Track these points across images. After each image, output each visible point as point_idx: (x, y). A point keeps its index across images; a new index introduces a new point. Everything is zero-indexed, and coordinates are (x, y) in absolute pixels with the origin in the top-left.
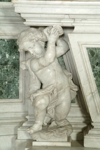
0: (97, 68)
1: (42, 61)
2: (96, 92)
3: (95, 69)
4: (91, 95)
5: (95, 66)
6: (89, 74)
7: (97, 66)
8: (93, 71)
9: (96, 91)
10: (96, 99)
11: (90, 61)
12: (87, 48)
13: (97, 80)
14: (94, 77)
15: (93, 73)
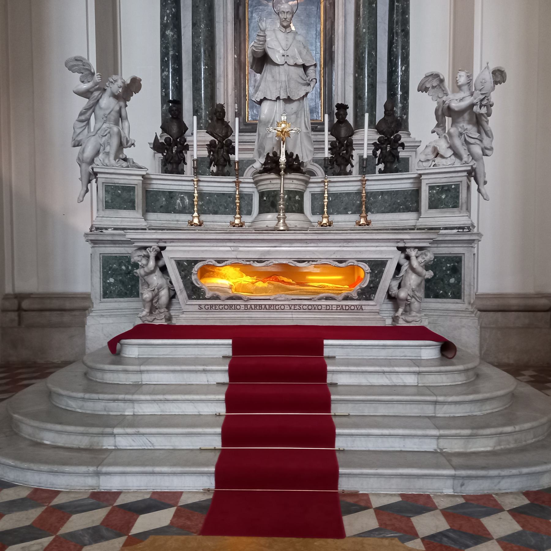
1: (146, 269)
12: (175, 260)
14: (182, 279)
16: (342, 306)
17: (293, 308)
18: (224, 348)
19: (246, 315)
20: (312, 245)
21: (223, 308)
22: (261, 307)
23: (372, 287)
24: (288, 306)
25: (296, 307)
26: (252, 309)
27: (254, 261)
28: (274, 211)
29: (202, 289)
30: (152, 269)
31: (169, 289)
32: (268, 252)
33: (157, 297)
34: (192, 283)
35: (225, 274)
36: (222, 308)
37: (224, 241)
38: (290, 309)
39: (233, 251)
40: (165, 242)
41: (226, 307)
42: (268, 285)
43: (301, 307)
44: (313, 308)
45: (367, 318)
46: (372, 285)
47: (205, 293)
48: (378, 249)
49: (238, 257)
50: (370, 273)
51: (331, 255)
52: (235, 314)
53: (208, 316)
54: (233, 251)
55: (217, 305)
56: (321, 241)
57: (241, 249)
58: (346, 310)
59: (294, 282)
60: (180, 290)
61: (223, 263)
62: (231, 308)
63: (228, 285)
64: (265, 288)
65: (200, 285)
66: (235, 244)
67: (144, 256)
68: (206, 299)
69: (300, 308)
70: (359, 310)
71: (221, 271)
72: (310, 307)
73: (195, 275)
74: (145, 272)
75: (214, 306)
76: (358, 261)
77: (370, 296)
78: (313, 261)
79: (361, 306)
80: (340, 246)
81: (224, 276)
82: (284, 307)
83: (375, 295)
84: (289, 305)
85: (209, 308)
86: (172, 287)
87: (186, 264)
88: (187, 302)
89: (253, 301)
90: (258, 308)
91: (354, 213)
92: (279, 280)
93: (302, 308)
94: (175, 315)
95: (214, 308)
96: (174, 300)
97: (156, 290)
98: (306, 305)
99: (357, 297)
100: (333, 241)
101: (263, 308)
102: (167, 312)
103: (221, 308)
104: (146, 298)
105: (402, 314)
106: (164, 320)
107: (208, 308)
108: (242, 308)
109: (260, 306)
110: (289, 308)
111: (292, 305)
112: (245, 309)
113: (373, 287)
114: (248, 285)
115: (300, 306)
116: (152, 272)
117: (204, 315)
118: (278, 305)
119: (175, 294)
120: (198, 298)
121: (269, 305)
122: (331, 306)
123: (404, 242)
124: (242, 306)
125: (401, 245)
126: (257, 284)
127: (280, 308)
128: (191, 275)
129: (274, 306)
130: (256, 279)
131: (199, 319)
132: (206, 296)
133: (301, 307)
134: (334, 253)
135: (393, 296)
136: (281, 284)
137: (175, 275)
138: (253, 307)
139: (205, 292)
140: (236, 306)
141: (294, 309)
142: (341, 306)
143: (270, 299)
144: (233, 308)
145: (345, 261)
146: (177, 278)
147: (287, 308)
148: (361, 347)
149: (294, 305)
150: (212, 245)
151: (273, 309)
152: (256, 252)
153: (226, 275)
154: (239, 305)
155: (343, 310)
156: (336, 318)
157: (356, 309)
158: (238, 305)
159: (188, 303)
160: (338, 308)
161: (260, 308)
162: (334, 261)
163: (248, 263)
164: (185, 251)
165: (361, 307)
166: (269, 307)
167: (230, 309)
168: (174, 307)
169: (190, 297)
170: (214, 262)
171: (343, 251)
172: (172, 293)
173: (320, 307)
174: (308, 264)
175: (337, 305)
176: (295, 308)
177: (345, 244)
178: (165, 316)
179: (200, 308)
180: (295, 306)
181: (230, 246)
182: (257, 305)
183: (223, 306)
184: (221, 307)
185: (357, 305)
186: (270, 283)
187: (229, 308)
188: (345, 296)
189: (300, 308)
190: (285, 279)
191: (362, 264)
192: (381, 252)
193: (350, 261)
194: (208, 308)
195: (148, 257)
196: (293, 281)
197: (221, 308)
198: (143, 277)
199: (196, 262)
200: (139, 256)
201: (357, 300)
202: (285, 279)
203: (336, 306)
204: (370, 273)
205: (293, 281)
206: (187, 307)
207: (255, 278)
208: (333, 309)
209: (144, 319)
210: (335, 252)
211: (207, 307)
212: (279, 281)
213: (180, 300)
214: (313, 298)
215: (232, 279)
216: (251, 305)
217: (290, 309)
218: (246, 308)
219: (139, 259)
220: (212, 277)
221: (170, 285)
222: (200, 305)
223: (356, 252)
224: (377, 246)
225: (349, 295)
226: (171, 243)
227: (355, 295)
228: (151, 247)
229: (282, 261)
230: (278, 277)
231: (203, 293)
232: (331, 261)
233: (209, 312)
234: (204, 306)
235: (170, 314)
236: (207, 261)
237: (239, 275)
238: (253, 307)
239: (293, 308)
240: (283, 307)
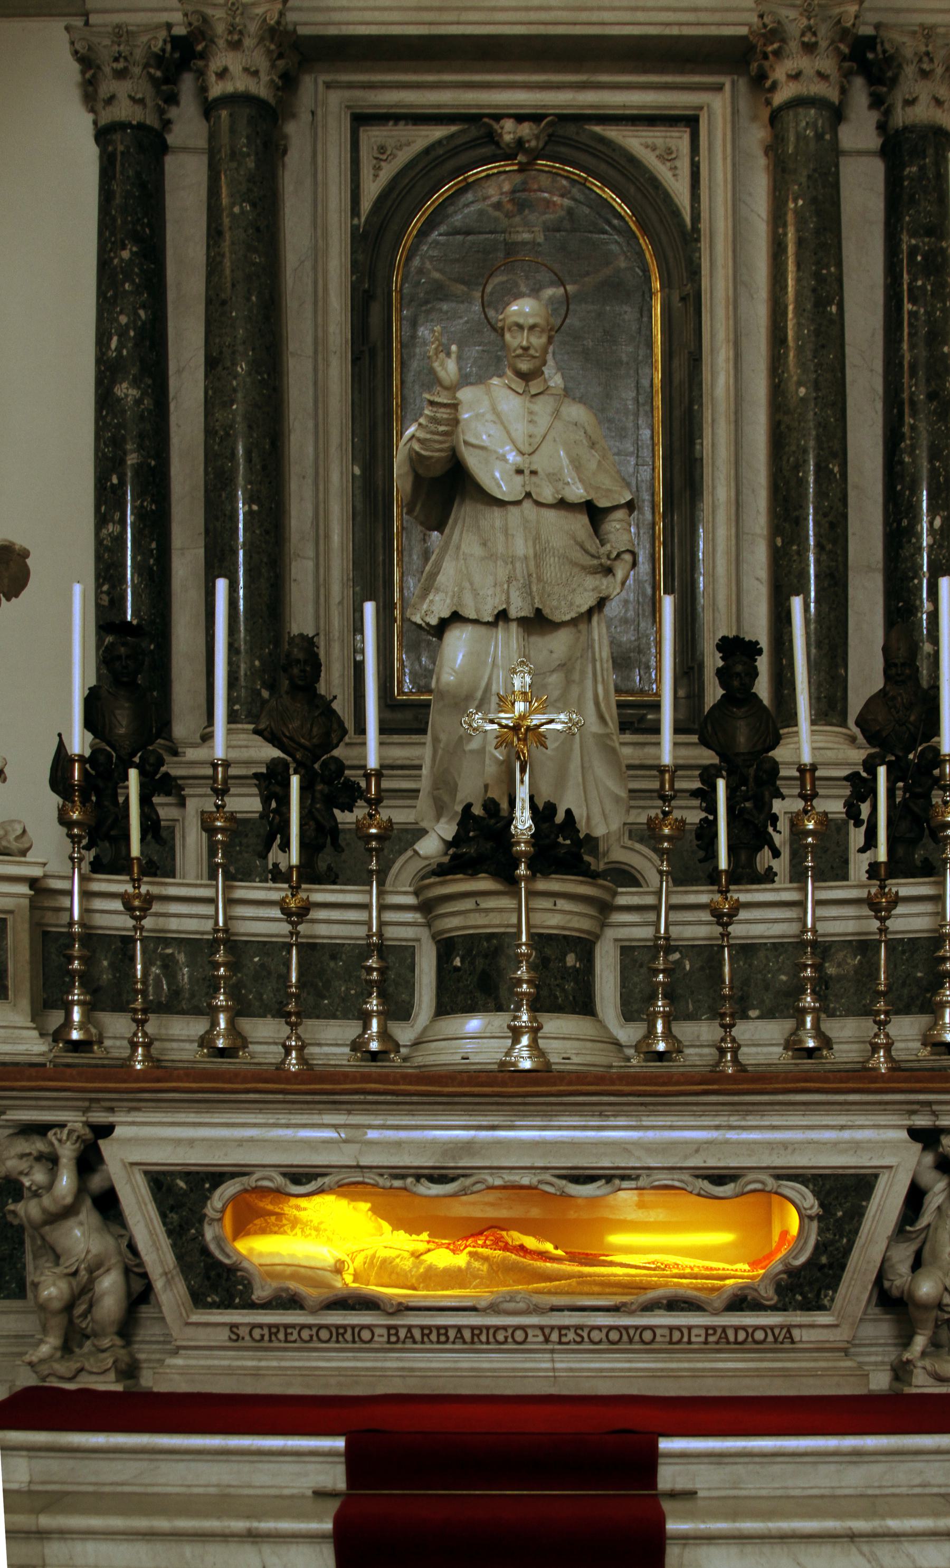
13: (174, 1246)
17: (555, 1336)
19: (392, 1361)
30: (69, 1200)
32: (468, 1147)
33: (86, 1298)
34: (205, 1251)
38: (547, 1340)
40: (111, 1110)
46: (824, 1260)
48: (846, 1135)
50: (820, 1218)
51: (686, 1157)
55: (293, 1326)
57: (372, 1134)
67: (40, 1158)
68: (252, 1306)
72: (614, 1336)
74: (44, 1211)
76: (778, 1177)
78: (623, 1178)
79: (789, 1328)
80: (717, 1128)
84: (542, 1328)
87: (182, 1184)
95: (281, 1336)
97: (83, 1273)
98: (599, 1328)
104: (50, 1299)
105: (924, 1354)
106: (112, 1376)
113: (830, 1266)
116: (68, 1212)
117: (249, 1361)
118: (505, 1328)
120: (227, 1304)
123: (934, 1114)
125: (922, 1121)
135: (895, 1293)
144: (348, 1336)
149: (560, 1328)
154: (369, 1327)
158: (363, 1327)
159: (194, 1318)
163: (397, 1183)
164: (178, 1142)
168: (147, 1332)
169: (198, 1300)
171: (727, 1142)
173: (648, 1335)
174: (606, 1189)
175: (707, 1328)
177: (734, 1120)
181: (335, 1127)
192: (856, 1146)
193: (751, 1176)
195: (51, 1161)
198: (37, 1227)
199: (217, 1177)
200: (22, 1156)
201: (774, 1308)
204: (820, 1218)
206: (190, 1331)
209: (45, 1369)
210: (699, 1147)
211: (257, 1333)
217: (547, 1340)
219: (23, 1165)
222: (233, 1327)
223: (771, 1146)
224: (842, 1128)
227: (769, 1294)
228: (62, 1126)
235: (131, 1355)
238: (417, 1334)
239: (555, 1336)
240: (519, 1335)
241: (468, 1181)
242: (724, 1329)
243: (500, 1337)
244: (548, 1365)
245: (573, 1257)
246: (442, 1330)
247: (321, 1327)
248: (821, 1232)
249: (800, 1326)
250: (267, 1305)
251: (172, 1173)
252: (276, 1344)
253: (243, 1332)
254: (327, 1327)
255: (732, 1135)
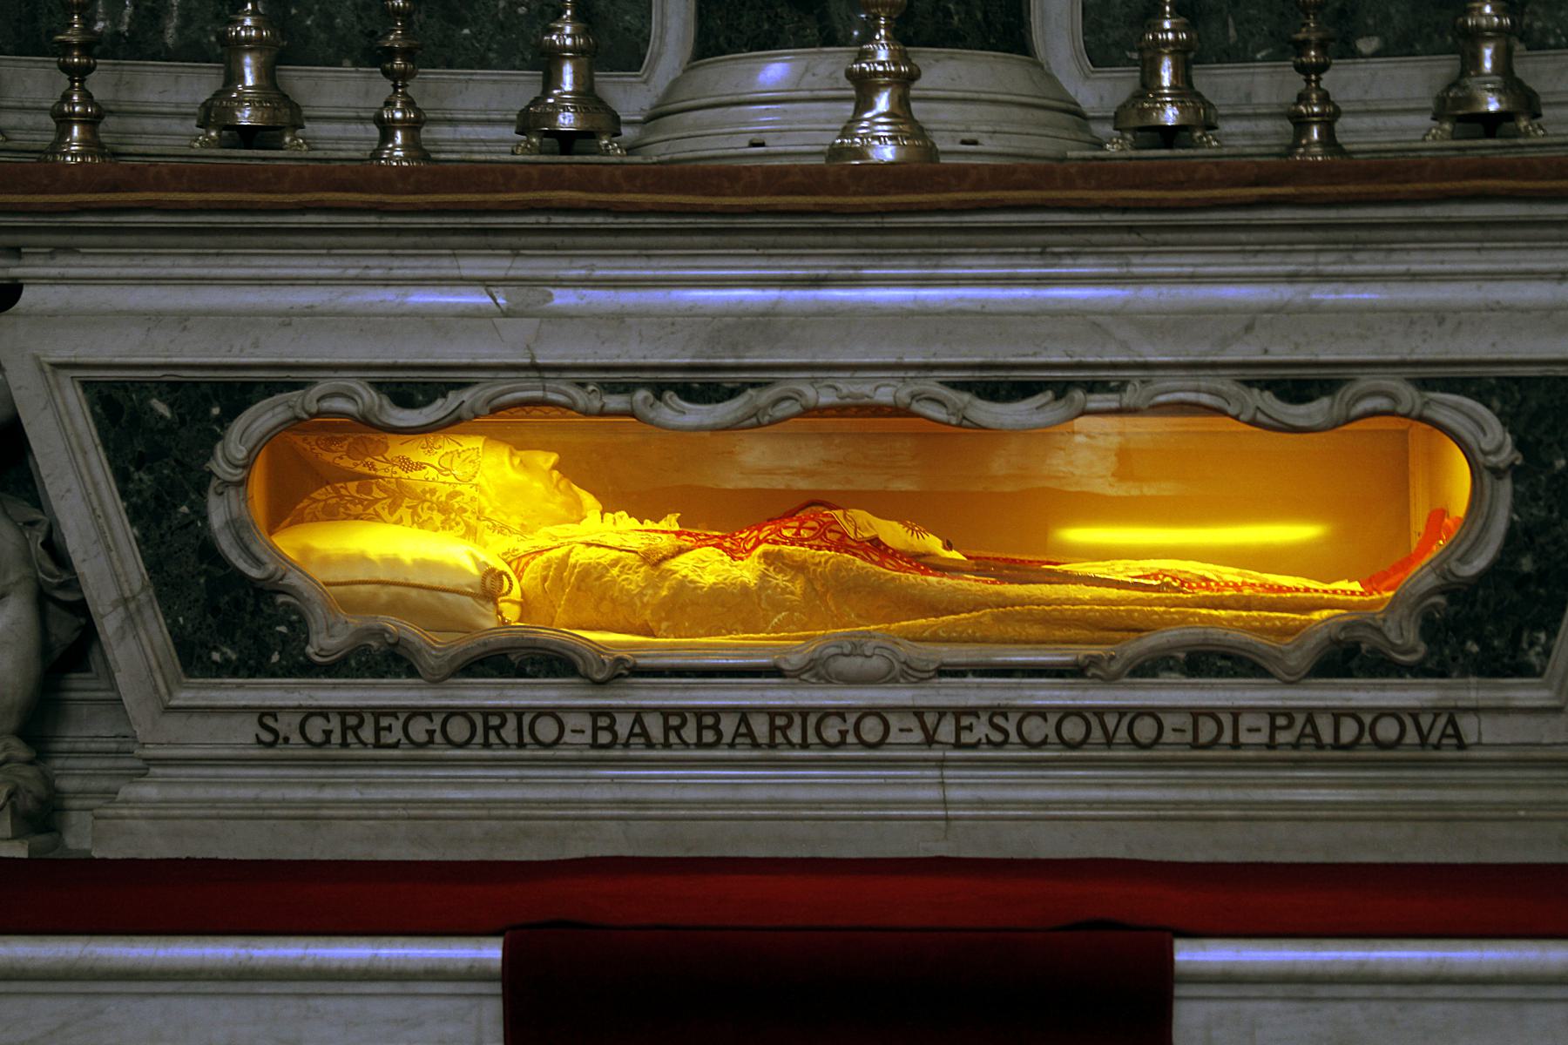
0: (141, 480)
2: (143, 597)
3: (131, 486)
4: (121, 609)
5: (132, 469)
6: (104, 511)
7: (138, 469)
8: (124, 494)
9: (143, 589)
10: (146, 630)
11: (106, 448)
12: (86, 385)
13: (143, 541)
14: (132, 522)
15: (121, 505)
16: (1310, 720)
17: (946, 731)
18: (443, 1004)
20: (1087, 267)
21: (438, 737)
22: (715, 727)
23: (1528, 576)
24: (913, 722)
25: (970, 728)
26: (650, 745)
27: (659, 389)
28: (812, 31)
29: (281, 599)
31: (42, 599)
34: (209, 552)
35: (453, 495)
36: (431, 733)
37: (437, 240)
38: (930, 740)
39: (506, 314)
41: (458, 729)
42: (763, 577)
43: (1011, 727)
44: (1097, 733)
45: (1497, 806)
46: (1527, 564)
47: (300, 627)
49: (539, 361)
50: (1516, 472)
51: (1225, 342)
52: (523, 782)
53: (328, 794)
54: (506, 314)
55: (392, 712)
56: (1150, 236)
57: (563, 299)
58: (1337, 745)
59: (955, 555)
60: (125, 601)
61: (429, 401)
62: (493, 738)
63: (474, 571)
64: (745, 588)
65: (271, 567)
66: (519, 262)
68: (308, 669)
69: (997, 737)
70: (1437, 747)
71: (420, 474)
72: (1073, 730)
73: (232, 492)
75: (369, 721)
76: (1424, 384)
77: (1515, 642)
79: (1452, 714)
80: (1292, 278)
81: (444, 509)
82: (880, 729)
83: (1553, 634)
84: (919, 713)
85: (336, 738)
86: (63, 586)
87: (162, 408)
88: (170, 693)
89: (655, 687)
90: (690, 733)
91: (1399, 47)
92: (844, 535)
93: (1014, 737)
94: (83, 793)
95: (367, 734)
96: (76, 680)
98: (1042, 712)
99: (1422, 648)
100: (1243, 237)
101: (727, 739)
102: (30, 762)
103: (423, 738)
107: (328, 733)
108: (578, 738)
109: (709, 721)
110: (917, 736)
111: (942, 712)
112: (595, 745)
114: (615, 571)
115: (999, 720)
117: (298, 789)
118: (840, 713)
119: (88, 634)
120: (253, 666)
121: (772, 713)
122: (1227, 720)
124: (571, 721)
126: (683, 566)
127: (851, 739)
128: (201, 488)
129: (812, 720)
130: (678, 534)
131: (258, 813)
132: (310, 650)
133: (1011, 727)
134: (1249, 328)
136: (858, 562)
137: (86, 497)
138: (655, 726)
139: (303, 620)
140: (527, 720)
141: (958, 745)
142: (1300, 720)
143: (774, 672)
144: (509, 733)
145: (1327, 387)
146: (97, 514)
147: (906, 733)
148: (1439, 991)
149: (959, 713)
150: (352, 272)
151: (805, 745)
152: (669, 321)
153: (456, 503)
154: (552, 712)
155: (1320, 746)
156: (1270, 804)
157: (1412, 736)
158: (541, 712)
159: (184, 697)
160: (1282, 737)
161: (709, 736)
162: (1249, 384)
163: (615, 402)
164: (155, 318)
165: (1452, 722)
166: (773, 728)
167: (487, 745)
170: (370, 398)
171: (1313, 309)
172: (64, 630)
173: (1145, 729)
174: (1059, 410)
175: (1273, 713)
176: (966, 737)
177: (1329, 263)
178: (10, 796)
179: (267, 737)
180: (965, 721)
182: (680, 712)
183: (438, 720)
184: (419, 729)
185: (1424, 710)
186: (779, 555)
187: (479, 739)
188: (1335, 642)
189: (997, 737)
190: (894, 533)
191: (1456, 408)
193: (1366, 382)
194: (328, 733)
196: (948, 546)
197: (423, 738)
201: (1419, 670)
202: (894, 533)
203: (1264, 722)
204: (1516, 472)
205: (948, 546)
206: (174, 726)
207: (671, 522)
208: (1244, 737)
211: (316, 728)
212: (842, 544)
213: (121, 678)
214: (1094, 661)
215: (502, 529)
216: (639, 713)
217: (930, 740)
218: (604, 738)
220: (357, 518)
221: (49, 565)
222: (265, 715)
223: (1408, 316)
225: (1359, 633)
226: (60, 260)
227: (1407, 639)
229: (867, 389)
230: (838, 513)
231: (291, 625)
232: (1226, 384)
233: (335, 762)
234: (298, 719)
235: (48, 780)
236: (316, 392)
237: (556, 504)
238: (655, 726)
239: (946, 731)
241: (765, 396)
242: (1311, 714)
243: (831, 734)
244: (933, 794)
245: (982, 567)
246: (708, 717)
247: (451, 713)
248: (1518, 503)
249: (1476, 710)
250: (337, 668)
251: (141, 385)
252: (356, 752)
253: (287, 725)
254: (463, 712)
255: (1324, 294)
